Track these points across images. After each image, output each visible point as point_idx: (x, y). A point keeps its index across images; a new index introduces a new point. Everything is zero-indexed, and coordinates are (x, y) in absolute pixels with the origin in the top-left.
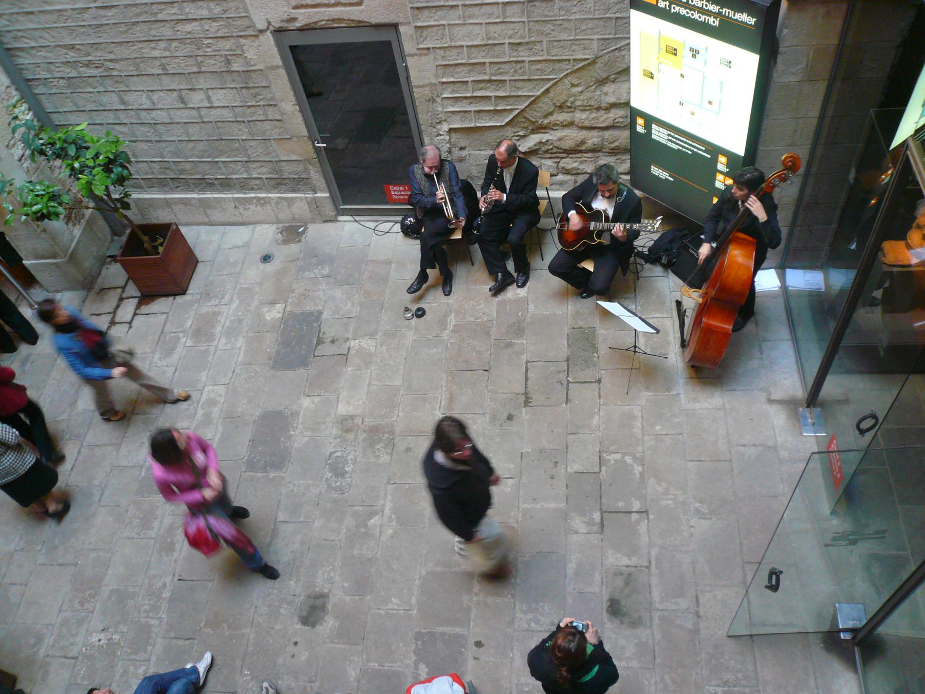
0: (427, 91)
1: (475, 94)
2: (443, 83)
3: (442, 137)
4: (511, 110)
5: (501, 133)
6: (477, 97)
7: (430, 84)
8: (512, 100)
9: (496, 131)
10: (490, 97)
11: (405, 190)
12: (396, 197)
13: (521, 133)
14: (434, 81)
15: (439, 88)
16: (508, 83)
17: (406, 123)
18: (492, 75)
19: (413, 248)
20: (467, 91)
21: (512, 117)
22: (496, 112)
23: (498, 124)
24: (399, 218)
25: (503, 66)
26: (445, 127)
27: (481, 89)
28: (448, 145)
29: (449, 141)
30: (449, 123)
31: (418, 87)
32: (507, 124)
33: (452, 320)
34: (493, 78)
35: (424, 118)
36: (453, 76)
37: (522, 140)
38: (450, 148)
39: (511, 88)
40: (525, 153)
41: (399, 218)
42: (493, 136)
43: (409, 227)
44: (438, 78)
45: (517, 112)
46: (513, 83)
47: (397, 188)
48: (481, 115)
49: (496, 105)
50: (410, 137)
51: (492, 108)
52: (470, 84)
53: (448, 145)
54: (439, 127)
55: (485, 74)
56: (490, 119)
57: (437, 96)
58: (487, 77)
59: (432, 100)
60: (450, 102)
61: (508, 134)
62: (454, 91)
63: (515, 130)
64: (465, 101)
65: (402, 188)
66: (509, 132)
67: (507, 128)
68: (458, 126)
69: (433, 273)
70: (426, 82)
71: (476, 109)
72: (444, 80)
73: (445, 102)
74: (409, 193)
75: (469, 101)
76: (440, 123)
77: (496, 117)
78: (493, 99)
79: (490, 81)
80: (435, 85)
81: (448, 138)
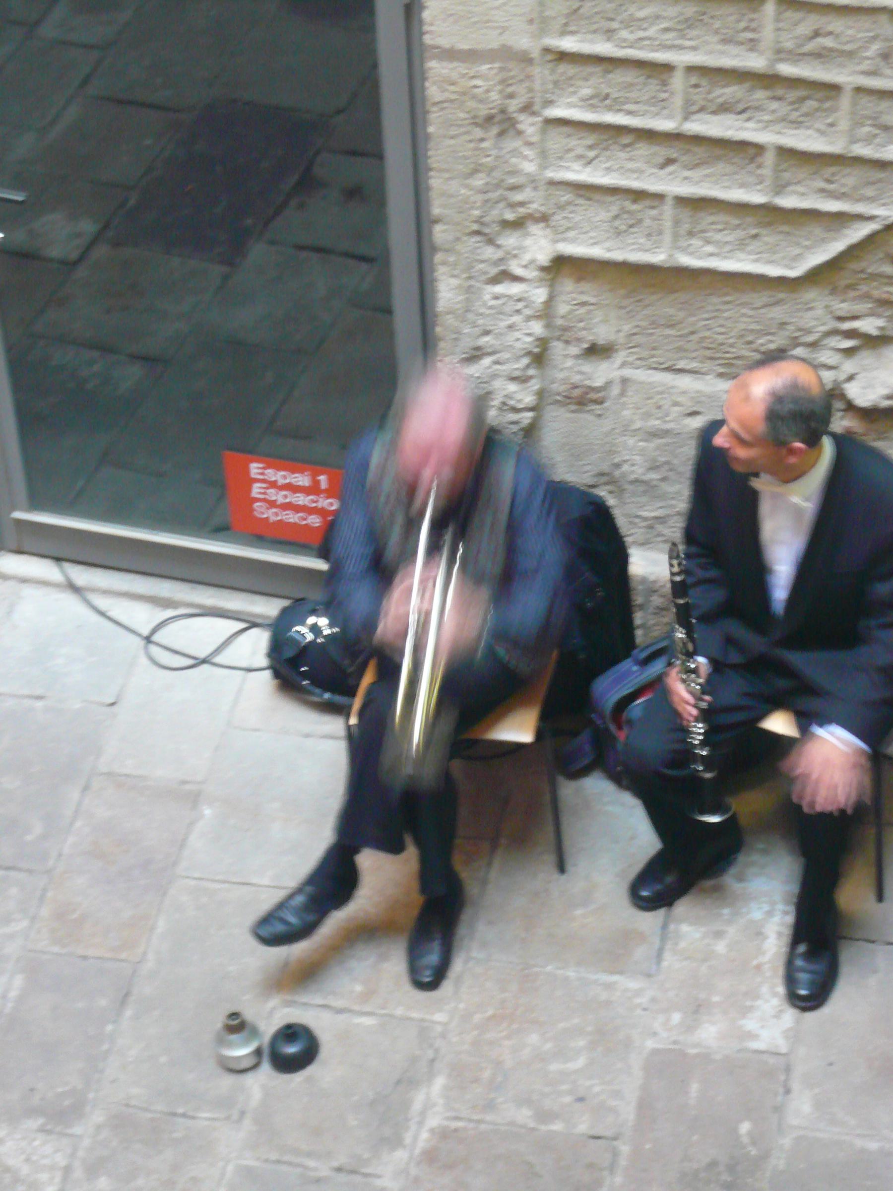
0: (484, 80)
1: (694, 127)
2: (563, 56)
3: (515, 289)
4: (842, 219)
5: (777, 313)
6: (698, 140)
7: (506, 54)
8: (849, 179)
9: (760, 298)
10: (759, 148)
11: (314, 490)
12: (272, 515)
13: (869, 325)
14: (524, 42)
15: (541, 73)
16: (845, 101)
17: (366, 195)
18: (781, 54)
19: (314, 751)
20: (660, 105)
21: (837, 246)
22: (771, 215)
23: (774, 271)
24: (270, 608)
25: (836, 24)
26: (539, 247)
27: (724, 108)
28: (537, 328)
29: (546, 313)
30: (559, 234)
31: (451, 55)
32: (815, 276)
33: (433, 1105)
34: (786, 69)
35: (452, 191)
36: (609, 34)
37: (866, 358)
38: (543, 343)
39: (857, 123)
40: (870, 414)
41: (270, 608)
42: (735, 319)
43: (305, 652)
44: (543, 31)
45: (858, 233)
46: (868, 105)
47: (280, 476)
48: (707, 219)
49: (780, 188)
50: (376, 260)
51: (757, 198)
52: (678, 81)
53: (537, 328)
54: (510, 240)
55: (753, 45)
56: (741, 245)
57: (527, 108)
58: (756, 62)
59: (502, 123)
60: (579, 143)
61: (808, 319)
62: (600, 100)
63: (843, 308)
64: (643, 150)
65: (303, 480)
66: (817, 311)
67: (810, 294)
68: (597, 252)
69: (384, 876)
70: (492, 41)
71: (686, 190)
72: (569, 44)
73: (557, 140)
74: (332, 504)
75: (663, 152)
76: (518, 224)
77: (769, 238)
78: (769, 158)
79: (768, 80)
80: (525, 59)
81: (540, 295)
